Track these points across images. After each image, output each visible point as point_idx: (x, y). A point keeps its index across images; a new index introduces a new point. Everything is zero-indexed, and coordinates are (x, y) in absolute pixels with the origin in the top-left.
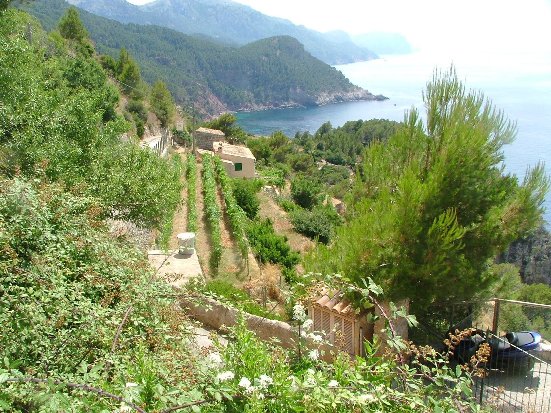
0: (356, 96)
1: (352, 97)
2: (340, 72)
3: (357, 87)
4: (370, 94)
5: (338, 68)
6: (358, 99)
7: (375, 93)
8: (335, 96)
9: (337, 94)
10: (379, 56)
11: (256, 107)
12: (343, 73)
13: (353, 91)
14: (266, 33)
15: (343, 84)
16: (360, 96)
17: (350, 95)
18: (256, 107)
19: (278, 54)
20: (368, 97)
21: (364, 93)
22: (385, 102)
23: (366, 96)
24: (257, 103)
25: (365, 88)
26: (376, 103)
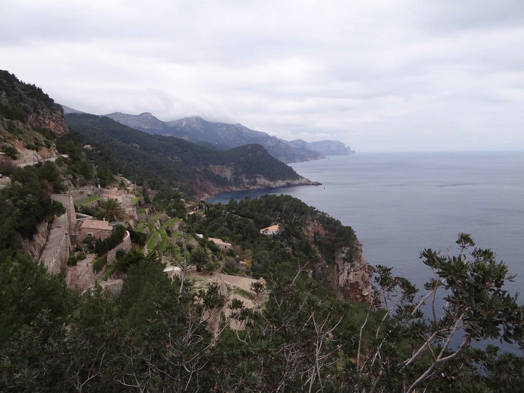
1: (298, 183)
4: (310, 181)
5: (289, 165)
6: (301, 184)
7: (313, 180)
10: (326, 157)
11: (234, 188)
13: (299, 179)
14: (245, 143)
15: (293, 175)
16: (303, 183)
17: (297, 182)
18: (234, 188)
19: (250, 155)
20: (308, 183)
23: (307, 183)
24: (236, 186)
26: (313, 186)
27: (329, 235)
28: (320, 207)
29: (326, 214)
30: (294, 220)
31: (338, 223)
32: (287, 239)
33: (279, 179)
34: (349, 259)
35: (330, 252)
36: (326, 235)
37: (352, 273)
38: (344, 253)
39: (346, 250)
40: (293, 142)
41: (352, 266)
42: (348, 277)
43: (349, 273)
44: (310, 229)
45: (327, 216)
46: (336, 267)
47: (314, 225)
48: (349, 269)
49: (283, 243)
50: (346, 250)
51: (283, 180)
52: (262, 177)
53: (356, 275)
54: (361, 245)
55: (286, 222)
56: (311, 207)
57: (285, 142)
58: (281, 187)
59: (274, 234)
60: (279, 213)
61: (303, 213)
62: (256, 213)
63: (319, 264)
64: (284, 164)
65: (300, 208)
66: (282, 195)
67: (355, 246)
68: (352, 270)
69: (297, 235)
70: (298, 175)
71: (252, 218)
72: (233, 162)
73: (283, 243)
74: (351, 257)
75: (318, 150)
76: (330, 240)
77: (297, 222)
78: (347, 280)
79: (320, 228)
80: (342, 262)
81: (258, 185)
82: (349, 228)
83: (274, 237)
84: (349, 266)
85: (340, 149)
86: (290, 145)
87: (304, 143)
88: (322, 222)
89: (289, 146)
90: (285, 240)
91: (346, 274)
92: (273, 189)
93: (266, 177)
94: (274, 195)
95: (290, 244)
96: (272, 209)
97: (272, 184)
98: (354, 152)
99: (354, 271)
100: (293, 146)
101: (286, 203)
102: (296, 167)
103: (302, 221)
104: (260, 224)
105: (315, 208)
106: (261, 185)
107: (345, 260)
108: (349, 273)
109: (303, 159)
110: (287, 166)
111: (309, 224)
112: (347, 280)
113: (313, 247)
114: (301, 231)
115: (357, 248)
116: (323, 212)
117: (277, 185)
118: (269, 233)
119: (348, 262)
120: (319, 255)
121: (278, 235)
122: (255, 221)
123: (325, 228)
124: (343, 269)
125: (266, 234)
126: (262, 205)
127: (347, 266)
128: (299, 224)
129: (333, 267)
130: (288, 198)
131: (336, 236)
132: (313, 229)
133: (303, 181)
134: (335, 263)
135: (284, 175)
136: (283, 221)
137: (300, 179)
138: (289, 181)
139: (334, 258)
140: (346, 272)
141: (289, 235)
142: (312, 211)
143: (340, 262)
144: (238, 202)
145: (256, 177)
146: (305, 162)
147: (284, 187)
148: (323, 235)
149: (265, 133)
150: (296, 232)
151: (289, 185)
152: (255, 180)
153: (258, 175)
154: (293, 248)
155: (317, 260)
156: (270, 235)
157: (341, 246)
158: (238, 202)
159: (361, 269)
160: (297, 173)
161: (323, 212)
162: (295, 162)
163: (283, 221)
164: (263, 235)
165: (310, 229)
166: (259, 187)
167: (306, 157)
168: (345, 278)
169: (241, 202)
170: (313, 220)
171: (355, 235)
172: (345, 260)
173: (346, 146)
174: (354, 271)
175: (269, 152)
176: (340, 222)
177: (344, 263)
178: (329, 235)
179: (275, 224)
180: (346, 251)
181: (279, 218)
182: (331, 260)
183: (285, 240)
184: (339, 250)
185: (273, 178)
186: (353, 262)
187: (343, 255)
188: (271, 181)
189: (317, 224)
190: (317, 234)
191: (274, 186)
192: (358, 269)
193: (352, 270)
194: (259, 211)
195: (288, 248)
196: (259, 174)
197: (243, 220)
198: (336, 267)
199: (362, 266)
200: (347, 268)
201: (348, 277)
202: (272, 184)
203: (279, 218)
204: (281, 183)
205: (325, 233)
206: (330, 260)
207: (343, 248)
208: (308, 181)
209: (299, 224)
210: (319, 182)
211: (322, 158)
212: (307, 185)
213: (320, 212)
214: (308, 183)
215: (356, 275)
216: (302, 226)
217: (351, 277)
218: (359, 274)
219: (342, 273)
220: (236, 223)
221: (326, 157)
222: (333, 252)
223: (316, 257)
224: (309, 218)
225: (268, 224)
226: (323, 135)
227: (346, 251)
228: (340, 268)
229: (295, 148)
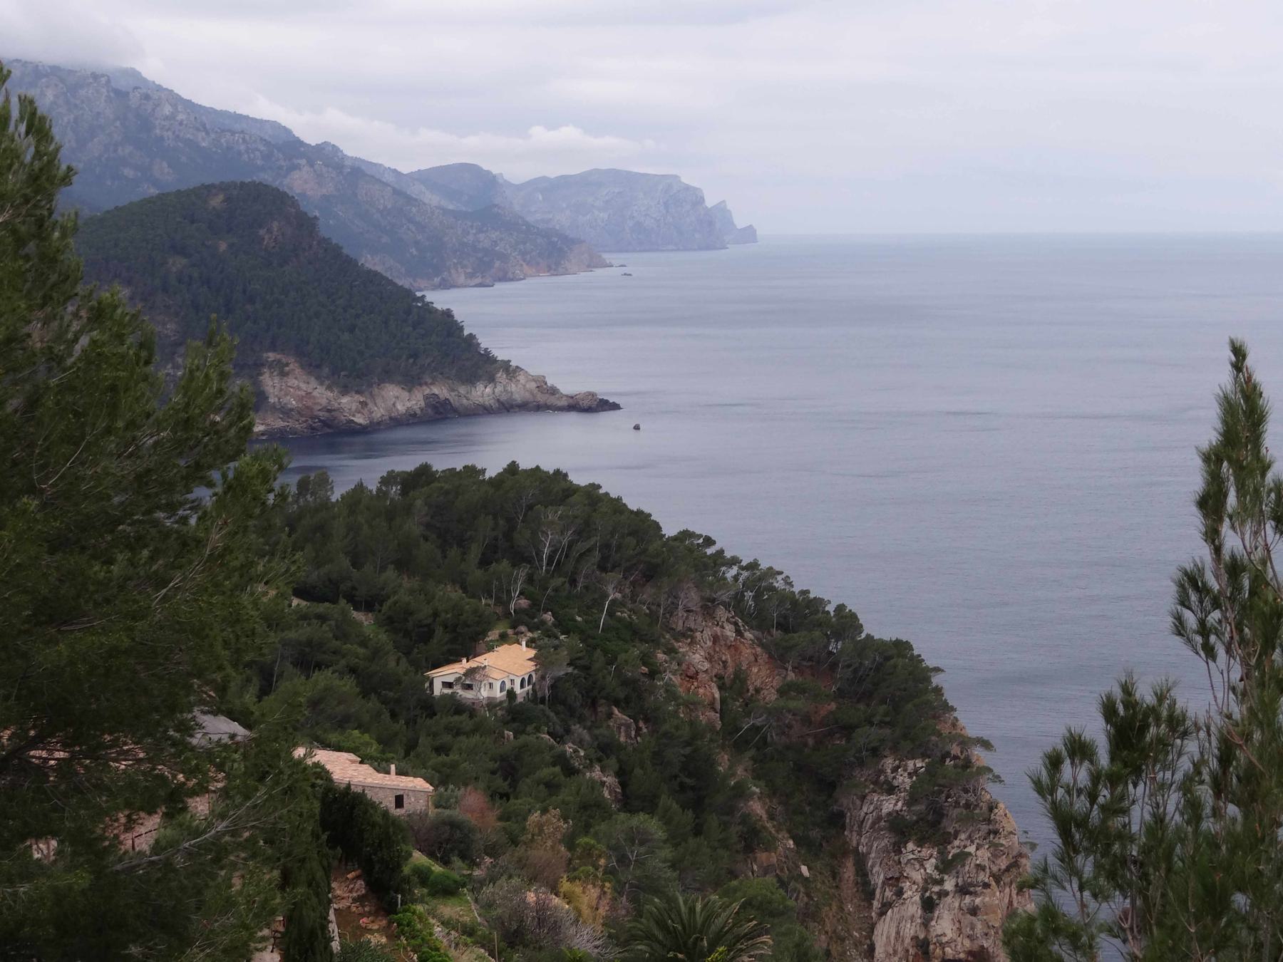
0: (504, 398)
2: (448, 314)
3: (506, 366)
4: (553, 391)
5: (439, 299)
6: (507, 408)
7: (569, 386)
8: (426, 398)
9: (436, 390)
12: (458, 316)
13: (492, 379)
15: (457, 353)
17: (482, 393)
20: (547, 402)
21: (533, 385)
22: (606, 417)
23: (541, 398)
25: (534, 371)
26: (573, 417)
27: (801, 690)
28: (742, 535)
29: (772, 573)
30: (611, 614)
31: (846, 622)
32: (581, 720)
33: (387, 376)
35: (816, 790)
36: (783, 692)
37: (952, 902)
38: (891, 790)
39: (905, 773)
40: (426, 178)
42: (926, 924)
43: (929, 905)
44: (701, 658)
45: (779, 583)
46: (849, 872)
47: (716, 639)
48: (929, 881)
49: (569, 748)
50: (905, 773)
51: (410, 382)
52: (293, 366)
53: (974, 911)
54: (986, 745)
55: (564, 625)
56: (686, 535)
57: (388, 178)
58: (397, 422)
59: (511, 694)
60: (522, 573)
61: (652, 573)
62: (390, 573)
63: (762, 856)
64: (408, 294)
67: (955, 750)
68: (949, 885)
69: (633, 698)
70: (488, 358)
71: (368, 605)
72: (128, 282)
73: (569, 748)
74: (939, 814)
75: (562, 220)
76: (807, 720)
77: (630, 626)
79: (747, 652)
80: (886, 841)
81: (274, 408)
82: (901, 647)
83: (514, 712)
84: (930, 866)
85: (673, 218)
86: (415, 190)
87: (489, 181)
88: (758, 620)
89: (410, 200)
90: (577, 728)
91: (912, 905)
92: (354, 431)
93: (312, 367)
94: (471, 471)
95: (604, 750)
96: (475, 552)
97: (348, 405)
98: (749, 234)
99: (963, 890)
100: (432, 199)
101: (552, 515)
103: (653, 616)
104: (427, 636)
105: (709, 541)
106: (286, 412)
107: (900, 830)
108: (929, 905)
109: (488, 268)
110: (428, 308)
111: (687, 635)
112: (923, 946)
113: (723, 761)
114: (653, 674)
115: (967, 764)
116: (753, 566)
117: (379, 412)
118: (484, 693)
119: (920, 843)
120: (757, 808)
121: (534, 698)
122: (390, 623)
123: (778, 656)
124: (895, 882)
126: (413, 526)
127: (920, 864)
128: (636, 634)
129: (834, 875)
130: (552, 487)
131: (841, 694)
132: (709, 658)
133: (518, 391)
134: (845, 851)
135: (415, 355)
136: (548, 617)
137: (501, 376)
138: (441, 391)
139: (836, 821)
140: (912, 896)
141: (593, 697)
142: (695, 557)
143: (873, 846)
145: (259, 365)
146: (500, 287)
147: (411, 420)
148: (770, 696)
149: (275, 125)
150: (625, 683)
151: (440, 413)
152: (257, 384)
153: (272, 356)
154: (623, 774)
155: (752, 839)
156: (492, 704)
157: (876, 753)
159: (998, 879)
160: (484, 342)
162: (446, 285)
163: (548, 617)
165: (697, 658)
166: (279, 424)
167: (503, 257)
168: (910, 930)
170: (708, 608)
171: (938, 691)
172: (900, 830)
174: (963, 890)
175: (326, 228)
176: (853, 616)
177: (898, 848)
178: (801, 690)
179: (503, 639)
180: (903, 780)
181: (524, 603)
182: (825, 831)
183: (577, 728)
184: (861, 775)
185: (353, 373)
186: (946, 839)
187: (890, 805)
188: (345, 390)
189: (729, 631)
190: (734, 685)
191: (360, 419)
192: (984, 877)
193: (949, 885)
194: (404, 564)
195: (596, 774)
196: (273, 348)
197: (322, 618)
198: (849, 872)
199: (1003, 863)
200: (918, 876)
201: (926, 924)
202: (348, 403)
203: (524, 603)
204: (396, 399)
205: (777, 682)
206: (815, 834)
207: (889, 763)
208: (541, 384)
209: (636, 634)
210: (602, 388)
211: (590, 266)
212: (539, 408)
213: (734, 561)
214: (547, 402)
215: (974, 911)
216: (655, 642)
217: (944, 925)
218: (989, 909)
219: (886, 906)
220: (292, 635)
221: (606, 256)
222: (829, 786)
223: (745, 819)
224: (691, 597)
225: (466, 640)
226: (569, 134)
227: (903, 780)
229: (445, 211)
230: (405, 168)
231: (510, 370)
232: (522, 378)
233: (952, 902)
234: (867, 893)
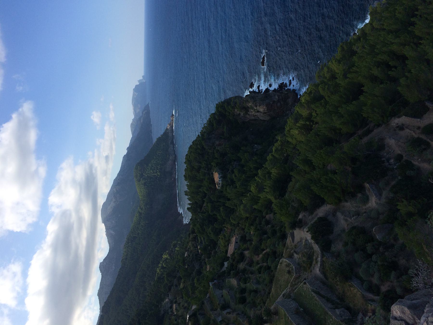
5: (155, 140)
17: (170, 134)
34: (246, 109)
38: (240, 114)
41: (253, 108)
42: (261, 112)
43: (258, 112)
59: (221, 177)
65: (199, 149)
66: (185, 163)
68: (256, 108)
78: (264, 113)
99: (256, 107)
102: (157, 132)
105: (199, 135)
108: (258, 112)
110: (156, 142)
116: (203, 128)
118: (221, 182)
124: (254, 116)
125: (221, 185)
137: (167, 131)
140: (257, 114)
144: (189, 202)
158: (189, 202)
161: (203, 128)
164: (222, 186)
168: (262, 115)
169: (189, 199)
173: (138, 84)
179: (212, 174)
186: (248, 107)
193: (256, 108)
200: (254, 113)
207: (235, 114)
217: (261, 110)
227: (238, 112)
228: (253, 118)
230: (131, 136)
231: (167, 129)
232: (168, 128)
233: (258, 108)
234: (255, 120)
